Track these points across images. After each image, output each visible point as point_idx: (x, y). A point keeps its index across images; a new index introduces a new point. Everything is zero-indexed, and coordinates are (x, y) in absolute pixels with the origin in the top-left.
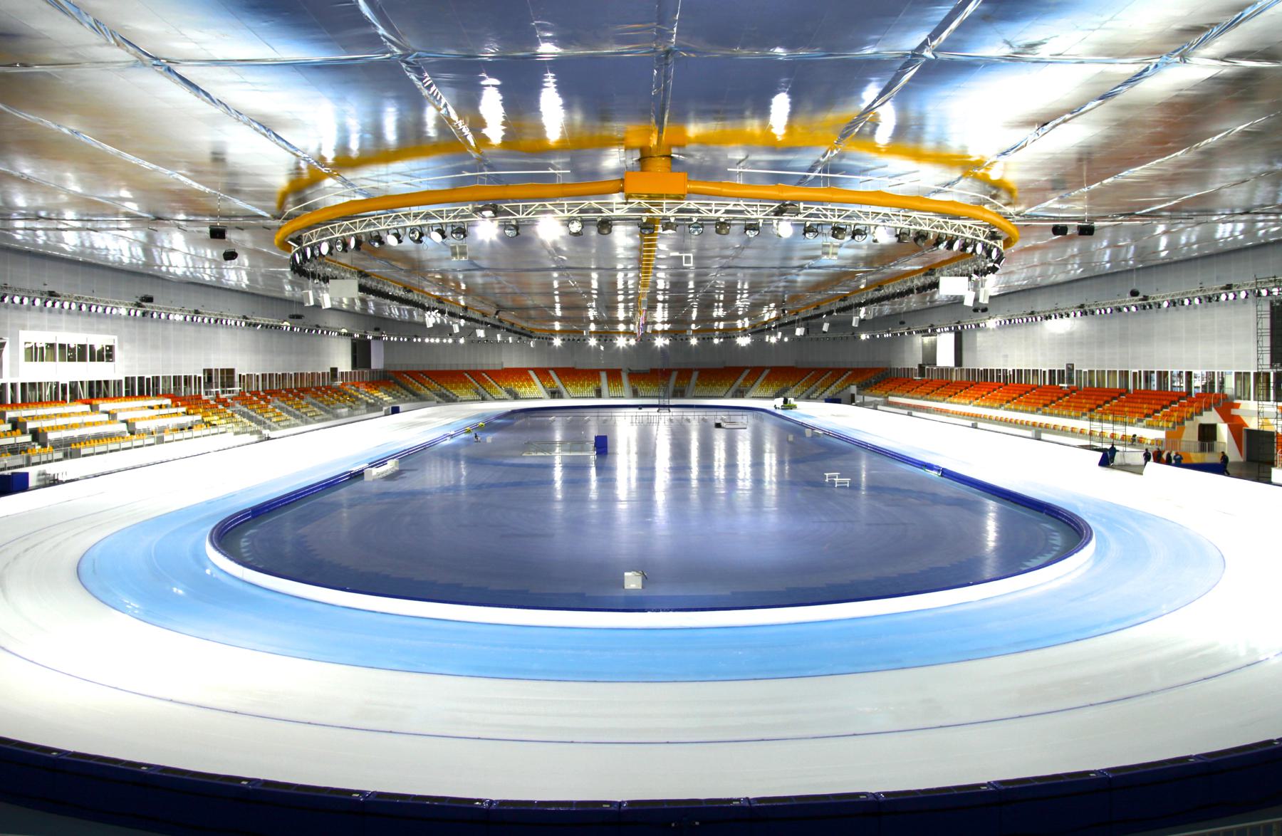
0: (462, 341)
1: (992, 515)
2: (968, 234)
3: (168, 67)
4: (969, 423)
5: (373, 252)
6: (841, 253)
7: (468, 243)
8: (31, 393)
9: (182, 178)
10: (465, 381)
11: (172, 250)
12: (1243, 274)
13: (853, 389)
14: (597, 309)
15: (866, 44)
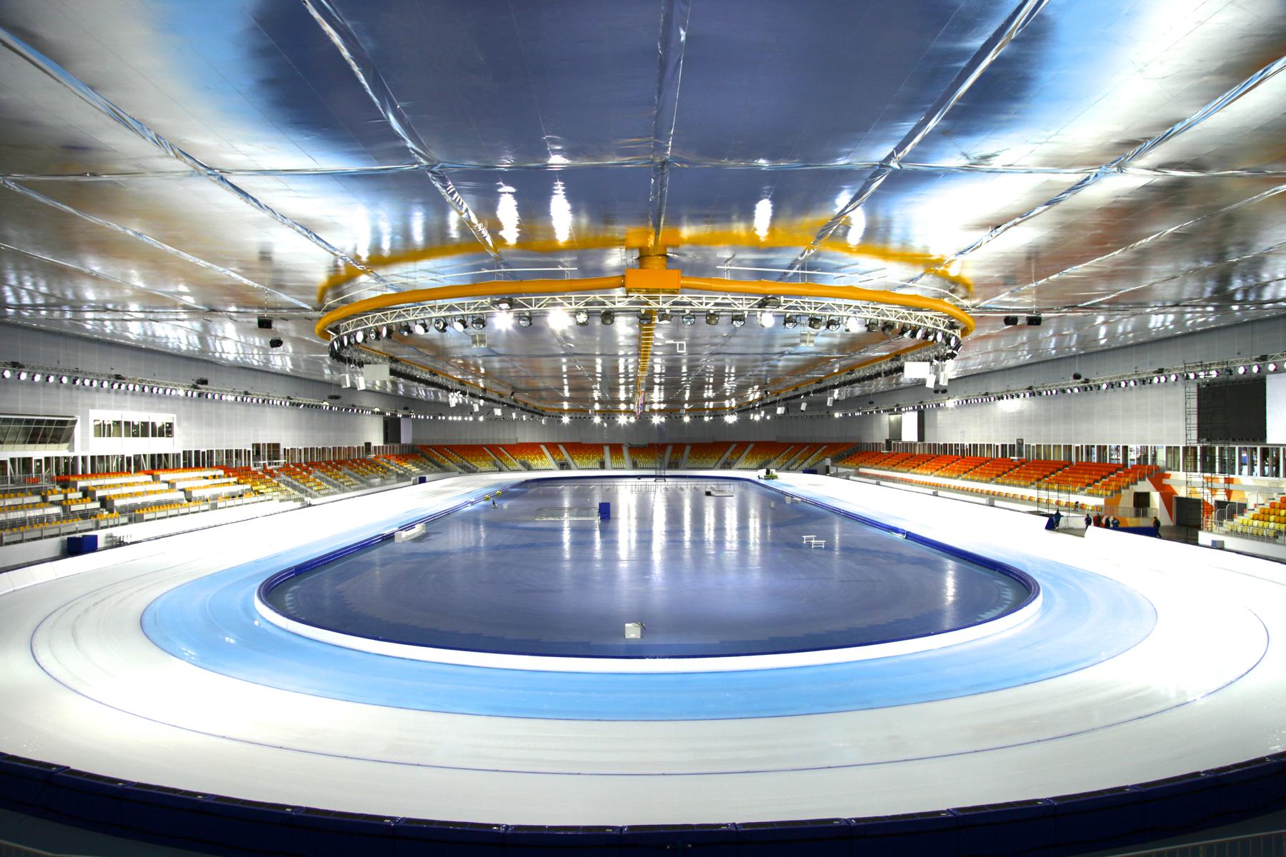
0: (481, 419)
1: (951, 572)
2: (930, 324)
3: (220, 176)
4: (931, 492)
5: (402, 341)
6: (817, 341)
7: (487, 332)
8: (99, 465)
9: (234, 275)
10: (483, 454)
11: (225, 338)
12: (1173, 360)
13: (828, 461)
14: (601, 390)
15: (839, 156)
